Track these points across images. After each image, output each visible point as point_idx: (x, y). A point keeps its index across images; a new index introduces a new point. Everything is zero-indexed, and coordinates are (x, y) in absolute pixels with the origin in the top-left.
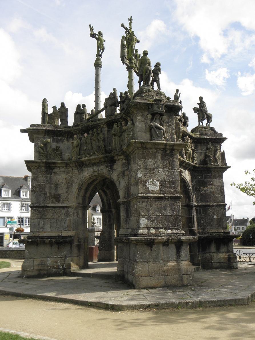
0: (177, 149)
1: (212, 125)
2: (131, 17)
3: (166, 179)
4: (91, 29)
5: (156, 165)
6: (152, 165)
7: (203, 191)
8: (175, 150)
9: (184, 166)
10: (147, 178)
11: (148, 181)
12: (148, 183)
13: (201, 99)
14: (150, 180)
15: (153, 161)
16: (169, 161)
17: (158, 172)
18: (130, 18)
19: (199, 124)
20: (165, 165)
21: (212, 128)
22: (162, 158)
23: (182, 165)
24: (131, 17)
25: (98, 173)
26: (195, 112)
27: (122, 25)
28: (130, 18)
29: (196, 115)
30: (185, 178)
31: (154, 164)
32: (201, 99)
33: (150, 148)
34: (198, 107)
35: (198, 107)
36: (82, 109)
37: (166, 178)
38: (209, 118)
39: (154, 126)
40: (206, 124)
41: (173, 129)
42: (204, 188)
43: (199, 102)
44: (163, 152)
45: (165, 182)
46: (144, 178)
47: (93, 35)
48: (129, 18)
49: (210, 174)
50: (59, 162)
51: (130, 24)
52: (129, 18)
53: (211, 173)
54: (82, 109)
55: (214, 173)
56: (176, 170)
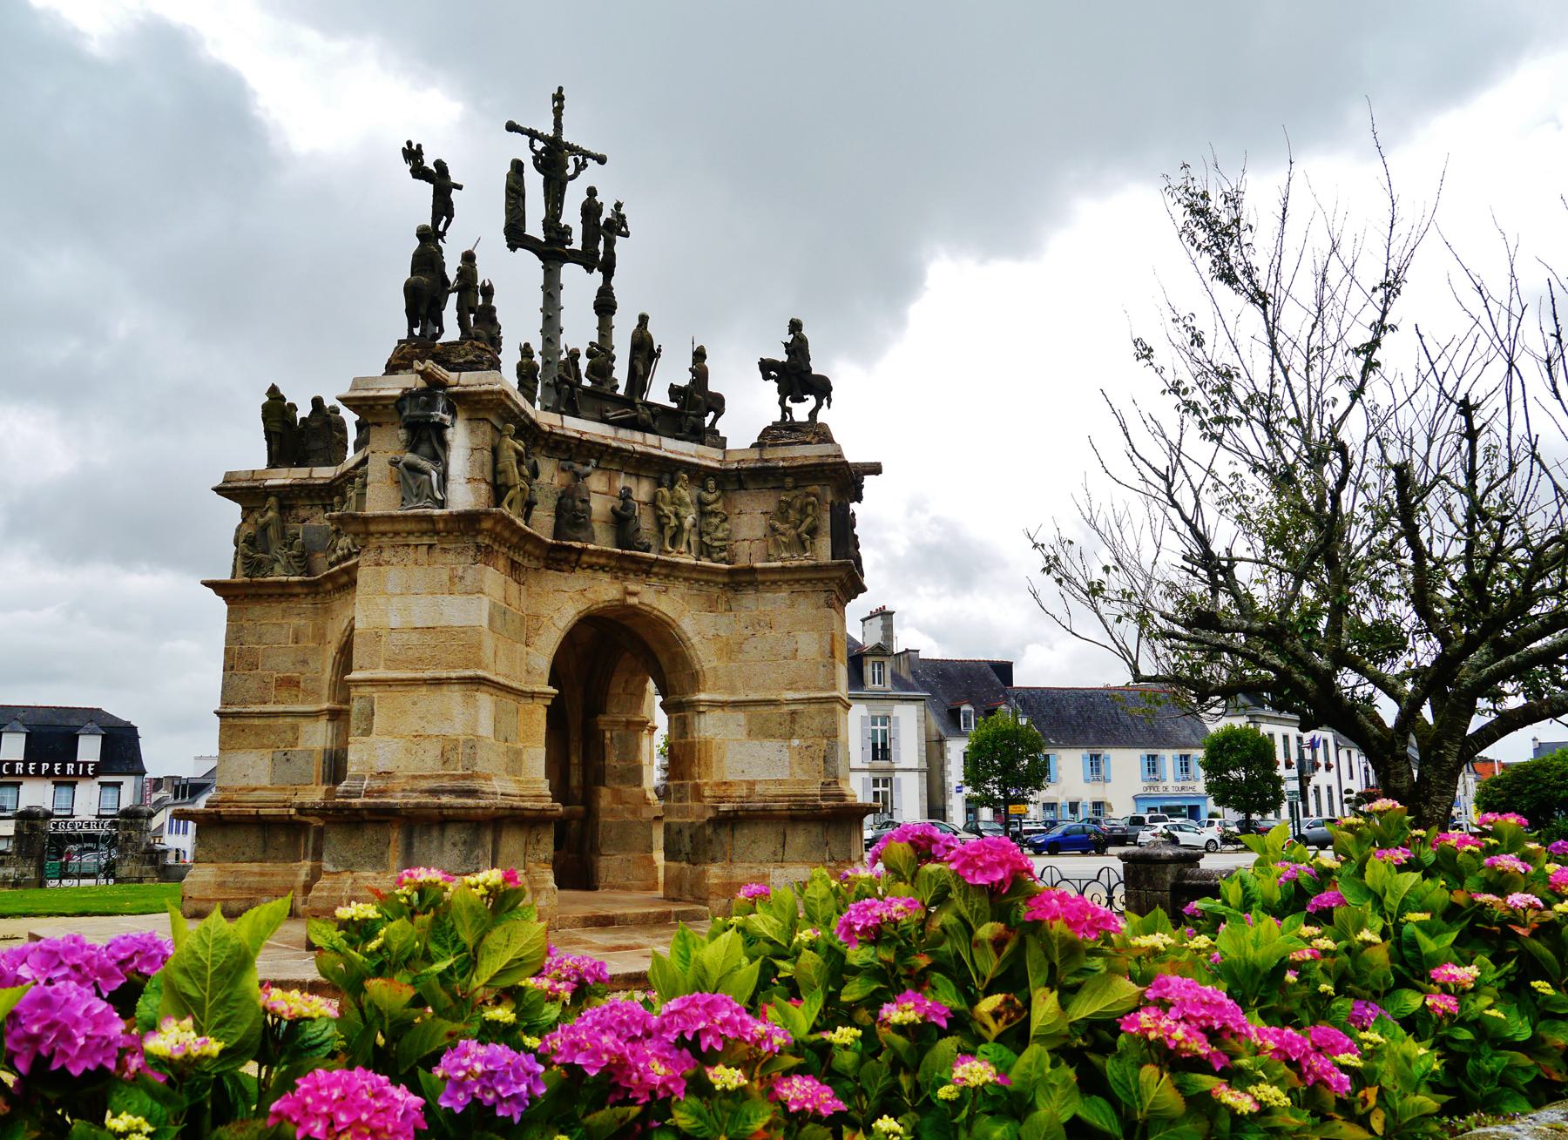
1: (822, 417)
2: (560, 89)
13: (795, 326)
19: (784, 417)
21: (824, 426)
24: (560, 89)
26: (766, 377)
27: (512, 127)
29: (772, 386)
32: (795, 326)
34: (782, 357)
35: (782, 357)
38: (822, 389)
40: (810, 415)
43: (789, 339)
47: (419, 172)
50: (296, 578)
51: (558, 112)
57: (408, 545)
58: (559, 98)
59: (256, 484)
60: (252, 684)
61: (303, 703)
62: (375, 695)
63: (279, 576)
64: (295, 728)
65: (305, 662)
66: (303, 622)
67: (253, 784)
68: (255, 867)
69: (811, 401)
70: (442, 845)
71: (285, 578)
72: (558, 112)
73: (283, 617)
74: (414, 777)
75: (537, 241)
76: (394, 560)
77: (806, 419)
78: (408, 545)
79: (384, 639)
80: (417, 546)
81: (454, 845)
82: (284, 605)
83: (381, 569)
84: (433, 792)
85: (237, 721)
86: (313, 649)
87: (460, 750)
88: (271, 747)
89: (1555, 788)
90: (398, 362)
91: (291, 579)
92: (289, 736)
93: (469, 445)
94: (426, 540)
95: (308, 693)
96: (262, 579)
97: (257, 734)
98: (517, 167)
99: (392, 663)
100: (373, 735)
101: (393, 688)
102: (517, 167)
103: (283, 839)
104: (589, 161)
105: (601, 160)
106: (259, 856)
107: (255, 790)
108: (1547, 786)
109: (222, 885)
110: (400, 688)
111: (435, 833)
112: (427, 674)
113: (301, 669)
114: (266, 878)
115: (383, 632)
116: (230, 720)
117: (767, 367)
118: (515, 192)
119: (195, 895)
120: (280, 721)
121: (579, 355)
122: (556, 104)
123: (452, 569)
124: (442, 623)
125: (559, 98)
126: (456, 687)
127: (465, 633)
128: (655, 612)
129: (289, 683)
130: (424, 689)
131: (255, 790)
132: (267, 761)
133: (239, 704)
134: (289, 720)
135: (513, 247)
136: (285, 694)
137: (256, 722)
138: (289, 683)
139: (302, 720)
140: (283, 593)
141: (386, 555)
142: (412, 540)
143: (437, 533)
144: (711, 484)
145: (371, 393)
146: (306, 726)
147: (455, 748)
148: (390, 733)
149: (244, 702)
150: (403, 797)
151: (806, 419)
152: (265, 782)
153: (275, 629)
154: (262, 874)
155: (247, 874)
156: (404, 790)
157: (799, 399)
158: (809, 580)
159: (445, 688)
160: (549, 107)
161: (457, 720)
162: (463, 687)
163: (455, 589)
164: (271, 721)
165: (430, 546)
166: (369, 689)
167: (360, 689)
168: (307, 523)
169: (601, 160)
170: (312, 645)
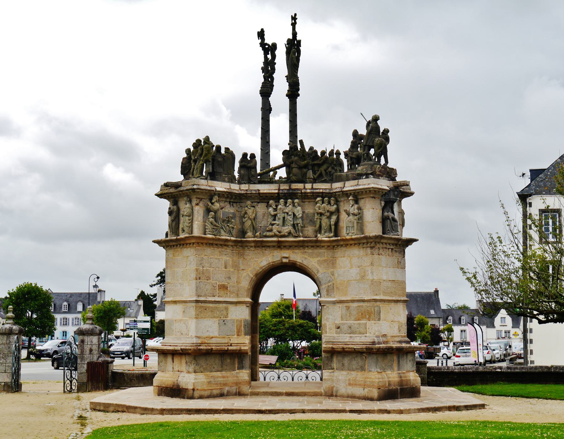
2: (295, 15)
4: (261, 34)
18: (293, 16)
24: (295, 15)
25: (289, 260)
28: (293, 16)
36: (249, 159)
39: (390, 217)
48: (292, 16)
51: (294, 25)
52: (292, 16)
54: (249, 159)
57: (386, 248)
58: (294, 18)
59: (213, 189)
60: (209, 287)
61: (230, 297)
62: (381, 305)
63: (224, 236)
64: (227, 309)
65: (229, 278)
66: (228, 258)
67: (212, 335)
68: (219, 374)
70: (407, 361)
71: (229, 238)
72: (294, 25)
73: (220, 256)
74: (392, 336)
76: (383, 253)
78: (386, 248)
79: (382, 284)
80: (389, 248)
81: (410, 361)
82: (220, 249)
83: (380, 256)
84: (400, 342)
85: (203, 305)
86: (233, 272)
87: (403, 327)
88: (218, 317)
89: (273, 330)
90: (379, 173)
91: (232, 238)
92: (225, 312)
93: (398, 211)
94: (392, 247)
95: (232, 293)
96: (219, 237)
97: (212, 311)
99: (385, 293)
100: (381, 320)
101: (385, 303)
103: (229, 361)
106: (220, 369)
107: (212, 338)
108: (270, 329)
109: (209, 383)
110: (387, 303)
111: (405, 357)
112: (394, 298)
113: (228, 281)
114: (225, 379)
115: (381, 281)
116: (200, 304)
119: (199, 388)
120: (221, 305)
121: (340, 154)
122: (293, 22)
123: (398, 259)
124: (396, 279)
125: (294, 18)
126: (401, 304)
127: (402, 283)
129: (223, 287)
130: (393, 304)
131: (212, 338)
132: (217, 324)
133: (203, 296)
134: (224, 305)
136: (222, 292)
137: (211, 305)
138: (223, 287)
139: (229, 305)
140: (224, 244)
141: (381, 251)
142: (388, 246)
143: (396, 245)
145: (380, 187)
146: (232, 308)
147: (402, 326)
148: (385, 320)
149: (205, 296)
150: (393, 344)
152: (216, 334)
153: (217, 261)
154: (224, 377)
155: (218, 377)
156: (392, 341)
159: (398, 303)
160: (290, 21)
161: (402, 316)
162: (403, 303)
163: (399, 266)
164: (217, 305)
165: (392, 249)
166: (379, 303)
167: (377, 303)
168: (223, 210)
170: (232, 270)
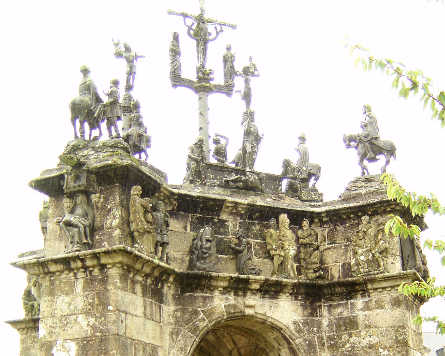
0: (109, 264)
3: (89, 335)
5: (72, 307)
6: (65, 307)
7: (348, 346)
8: (108, 266)
9: (258, 290)
10: (54, 337)
11: (56, 343)
12: (55, 347)
14: (58, 342)
15: (67, 299)
16: (98, 293)
17: (76, 320)
20: (90, 304)
22: (84, 289)
23: (251, 290)
30: (272, 318)
31: (69, 304)
33: (58, 271)
37: (90, 332)
41: (114, 218)
42: (350, 336)
44: (87, 276)
45: (88, 342)
46: (48, 338)
49: (365, 296)
53: (369, 296)
55: (376, 293)
56: (110, 311)
69: (382, 158)
75: (190, 81)
77: (379, 172)
98: (176, 37)
102: (176, 37)
104: (224, 28)
105: (233, 27)
117: (349, 140)
118: (175, 53)
128: (270, 320)
135: (175, 86)
144: (306, 223)
151: (379, 172)
157: (373, 160)
158: (384, 288)
169: (233, 27)
